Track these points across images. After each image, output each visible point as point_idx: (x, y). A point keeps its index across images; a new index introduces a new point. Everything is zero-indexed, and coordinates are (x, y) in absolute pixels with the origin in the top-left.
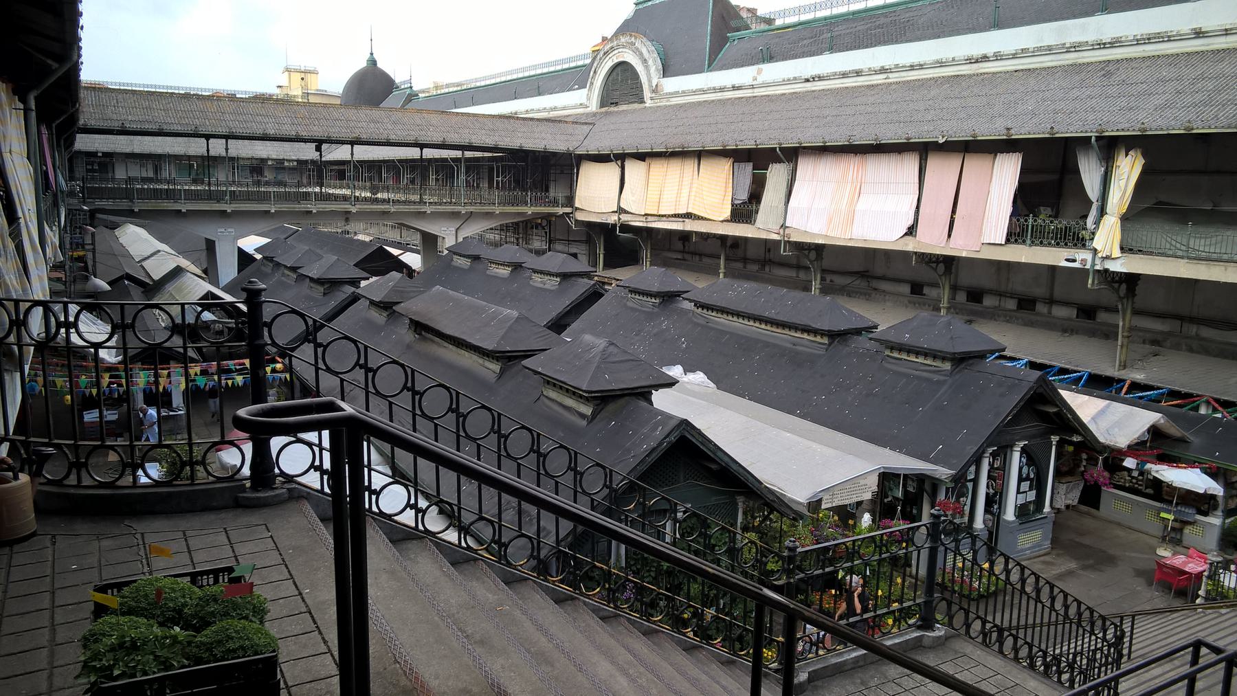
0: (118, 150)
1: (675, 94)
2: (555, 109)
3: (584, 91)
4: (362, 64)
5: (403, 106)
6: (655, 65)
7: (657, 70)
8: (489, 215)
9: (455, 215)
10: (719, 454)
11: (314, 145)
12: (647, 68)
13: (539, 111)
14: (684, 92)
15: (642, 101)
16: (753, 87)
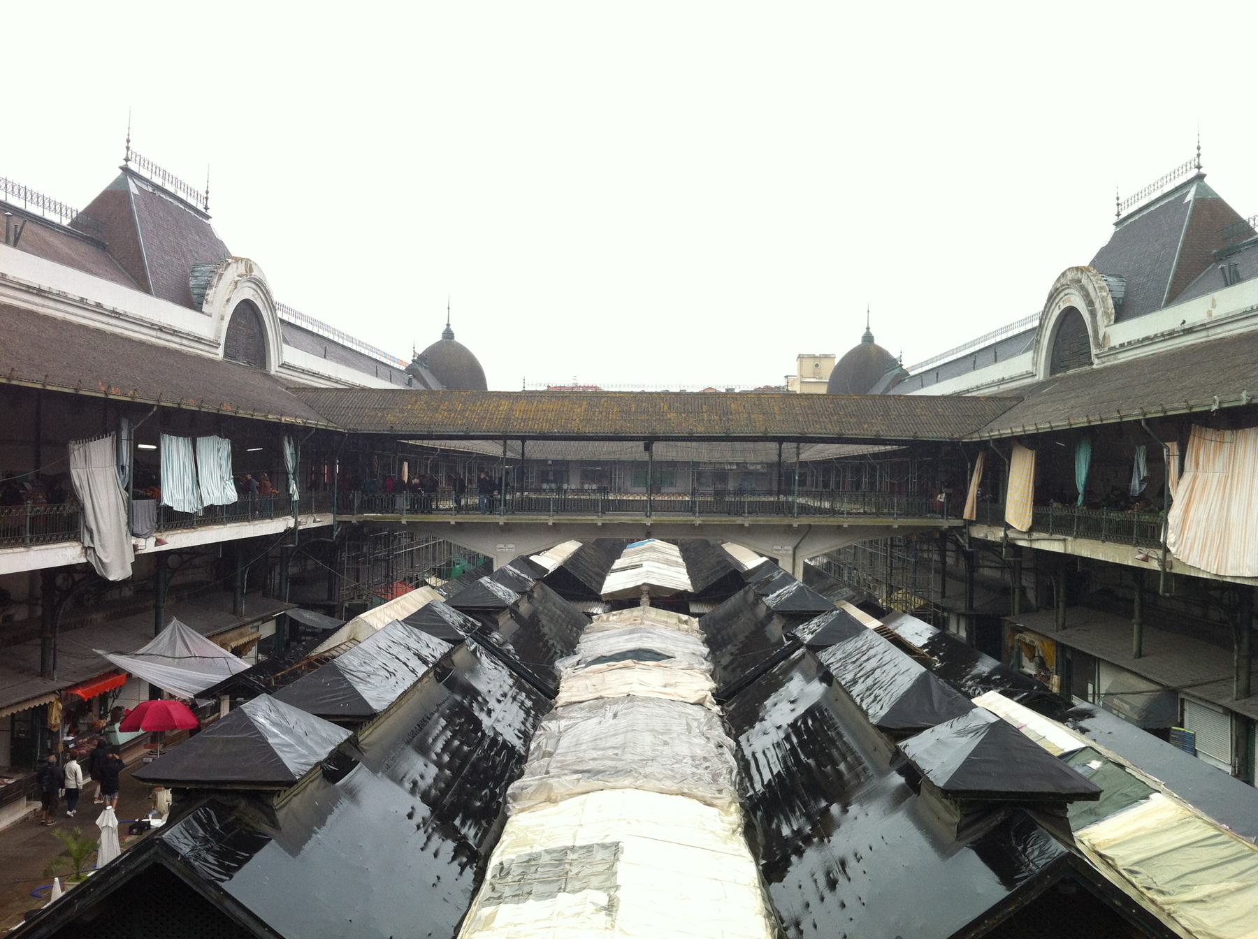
0: (569, 458)
1: (1130, 345)
2: (1002, 381)
3: (1030, 354)
4: (857, 341)
5: (888, 389)
6: (1105, 304)
7: (1106, 314)
8: (838, 530)
9: (788, 530)
10: (228, 903)
11: (641, 443)
12: (1093, 314)
13: (989, 385)
14: (1129, 343)
15: (1092, 364)
16: (1204, 327)
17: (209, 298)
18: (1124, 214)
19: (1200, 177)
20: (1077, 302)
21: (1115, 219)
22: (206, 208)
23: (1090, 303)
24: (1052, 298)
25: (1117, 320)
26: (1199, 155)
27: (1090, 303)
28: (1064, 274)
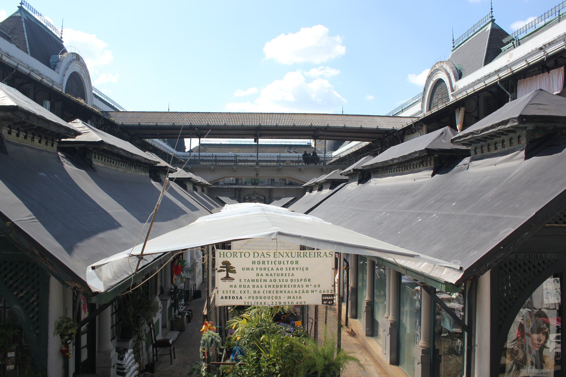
17: (58, 66)
18: (456, 46)
19: (493, 21)
20: (441, 75)
21: (453, 49)
22: (61, 38)
23: (448, 74)
24: (430, 77)
25: (460, 78)
26: (492, 12)
27: (448, 74)
28: (434, 66)
